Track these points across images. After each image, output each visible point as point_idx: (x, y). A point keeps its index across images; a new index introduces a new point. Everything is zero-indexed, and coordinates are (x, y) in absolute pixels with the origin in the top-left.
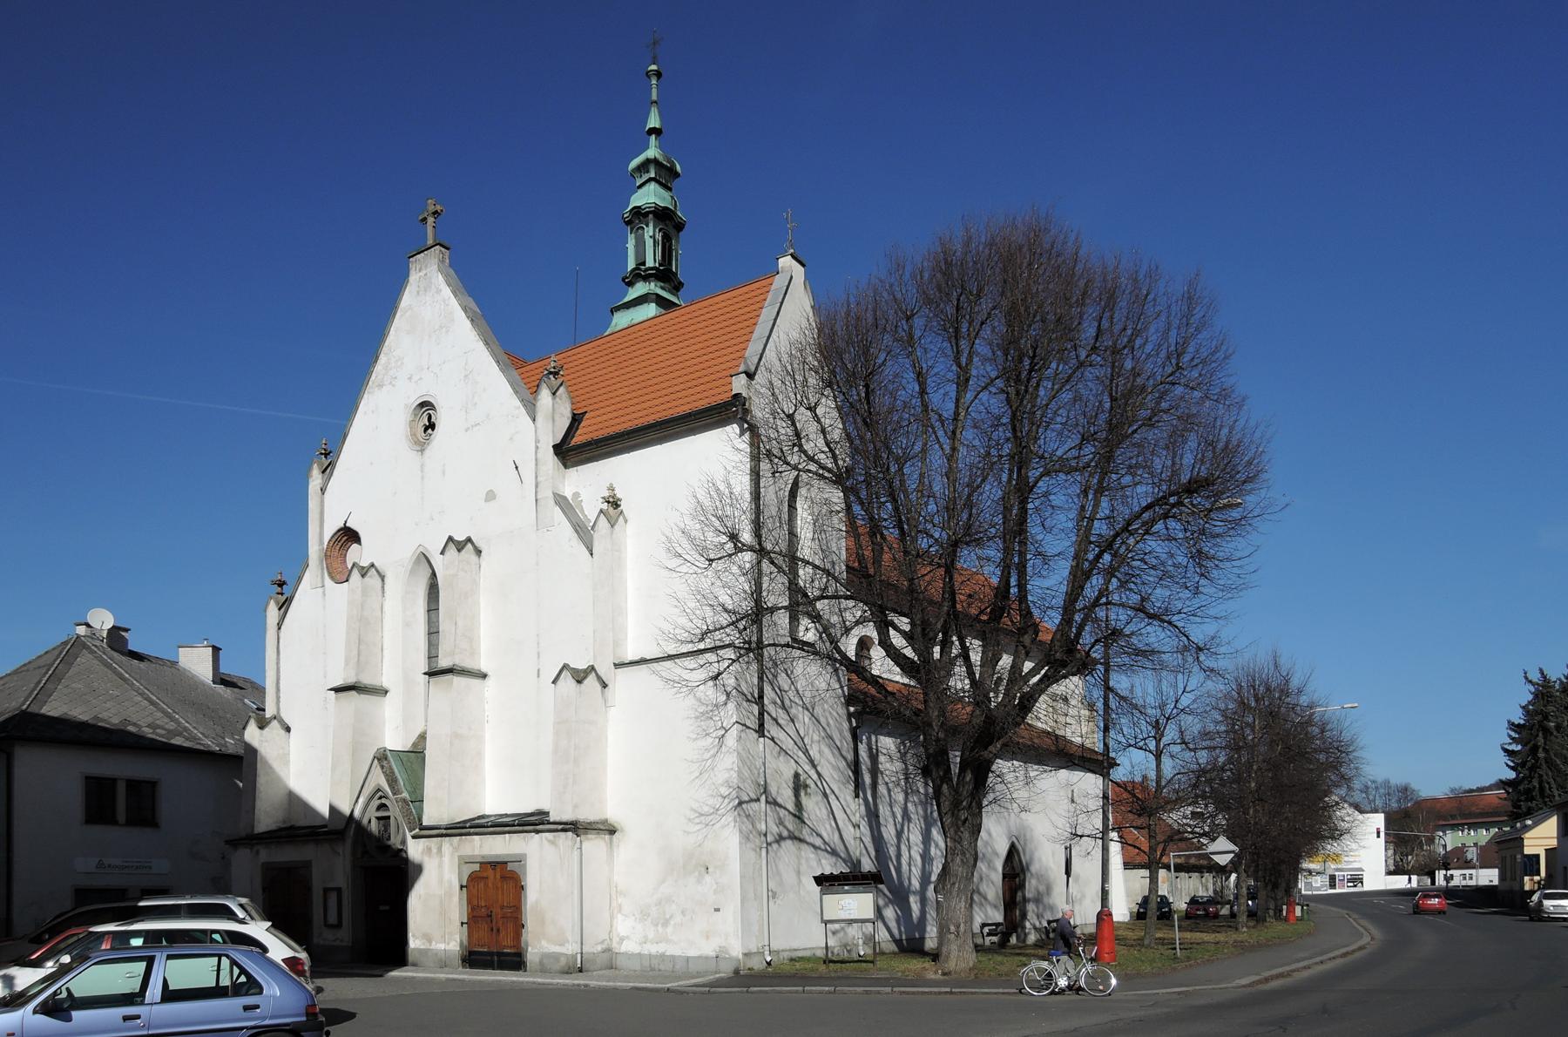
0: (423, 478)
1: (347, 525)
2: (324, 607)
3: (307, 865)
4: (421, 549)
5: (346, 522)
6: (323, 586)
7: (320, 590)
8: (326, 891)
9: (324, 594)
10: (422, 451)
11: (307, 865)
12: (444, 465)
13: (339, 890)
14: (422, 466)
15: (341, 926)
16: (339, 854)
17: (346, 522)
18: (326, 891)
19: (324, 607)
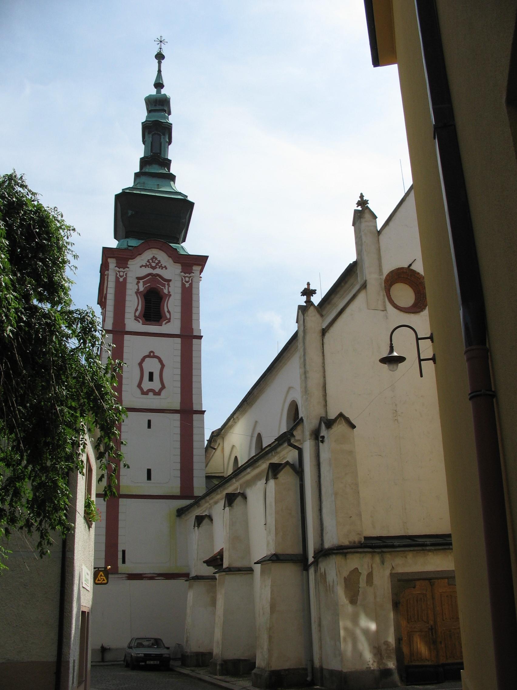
5: (410, 265)
17: (410, 265)
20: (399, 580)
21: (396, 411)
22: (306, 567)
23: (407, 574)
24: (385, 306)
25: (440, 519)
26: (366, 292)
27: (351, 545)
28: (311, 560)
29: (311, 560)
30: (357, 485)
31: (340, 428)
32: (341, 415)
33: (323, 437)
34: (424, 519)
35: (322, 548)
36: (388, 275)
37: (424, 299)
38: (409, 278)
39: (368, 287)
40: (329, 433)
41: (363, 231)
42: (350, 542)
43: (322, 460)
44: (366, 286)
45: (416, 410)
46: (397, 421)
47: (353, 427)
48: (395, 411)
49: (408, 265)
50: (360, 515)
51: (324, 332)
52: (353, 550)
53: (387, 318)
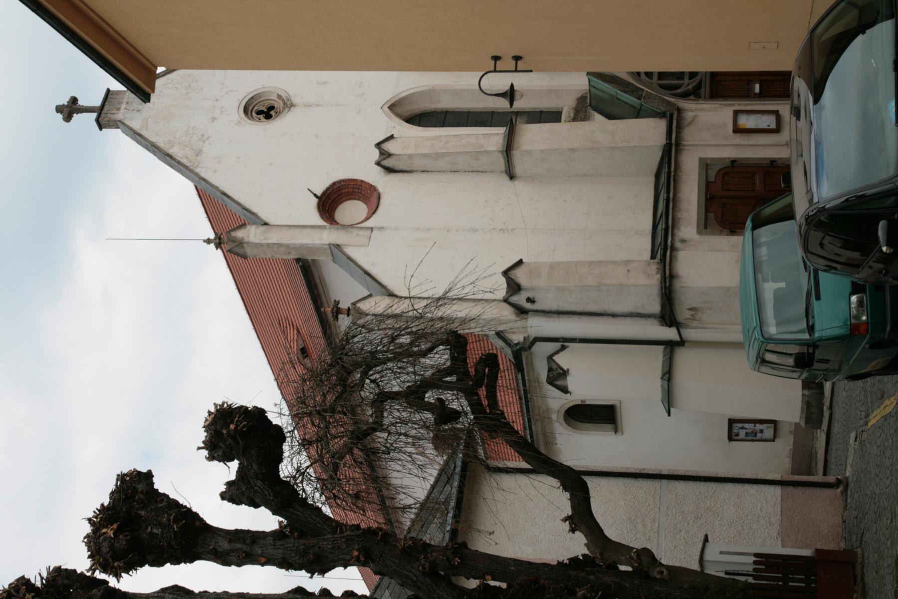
0: (318, 105)
1: (319, 193)
2: (396, 229)
3: (705, 165)
4: (386, 108)
5: (315, 195)
6: (372, 229)
7: (375, 232)
8: (737, 130)
9: (381, 228)
10: (292, 105)
11: (705, 165)
12: (318, 83)
13: (736, 113)
14: (307, 105)
15: (778, 111)
16: (694, 117)
17: (315, 195)
18: (737, 130)
19: (396, 229)
20: (706, 228)
21: (501, 230)
22: (682, 343)
23: (698, 219)
24: (367, 228)
25: (636, 197)
26: (345, 245)
27: (660, 272)
28: (670, 334)
29: (670, 334)
30: (591, 263)
31: (520, 276)
32: (506, 273)
33: (529, 300)
34: (634, 213)
35: (660, 318)
36: (325, 221)
37: (360, 187)
38: (330, 201)
39: (338, 243)
40: (526, 288)
41: (262, 241)
42: (658, 273)
43: (554, 307)
44: (337, 245)
45: (503, 209)
46: (514, 229)
47: (520, 262)
48: (501, 231)
49: (315, 198)
50: (627, 262)
51: (391, 295)
52: (667, 268)
53: (383, 228)
